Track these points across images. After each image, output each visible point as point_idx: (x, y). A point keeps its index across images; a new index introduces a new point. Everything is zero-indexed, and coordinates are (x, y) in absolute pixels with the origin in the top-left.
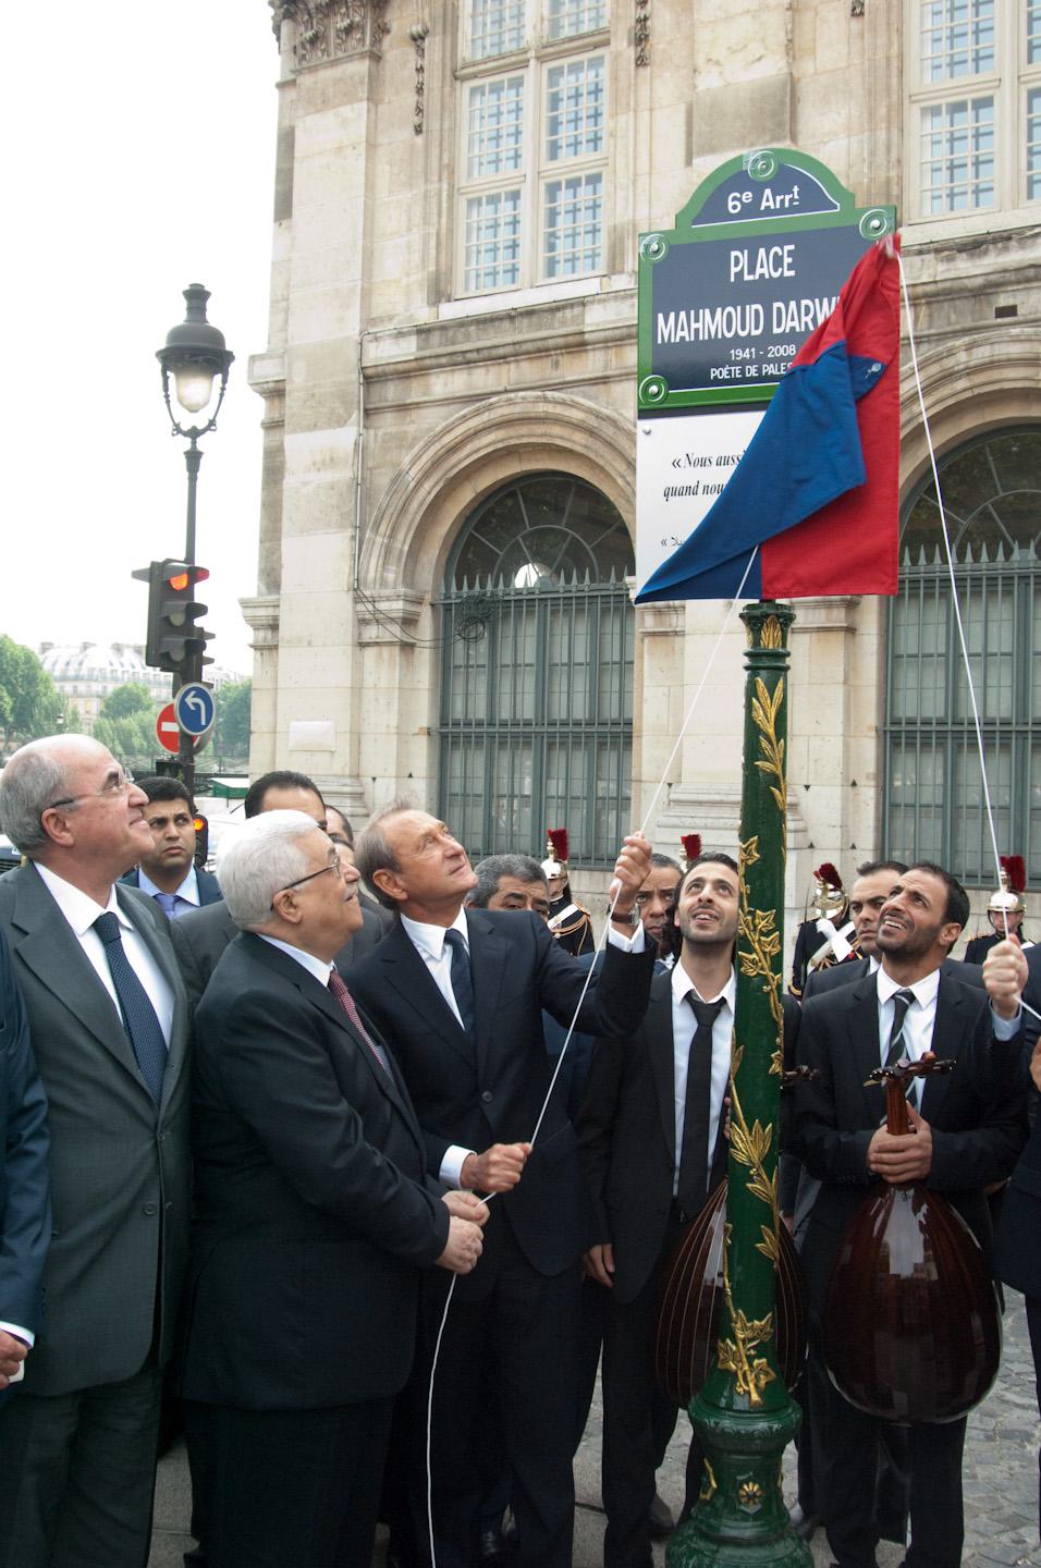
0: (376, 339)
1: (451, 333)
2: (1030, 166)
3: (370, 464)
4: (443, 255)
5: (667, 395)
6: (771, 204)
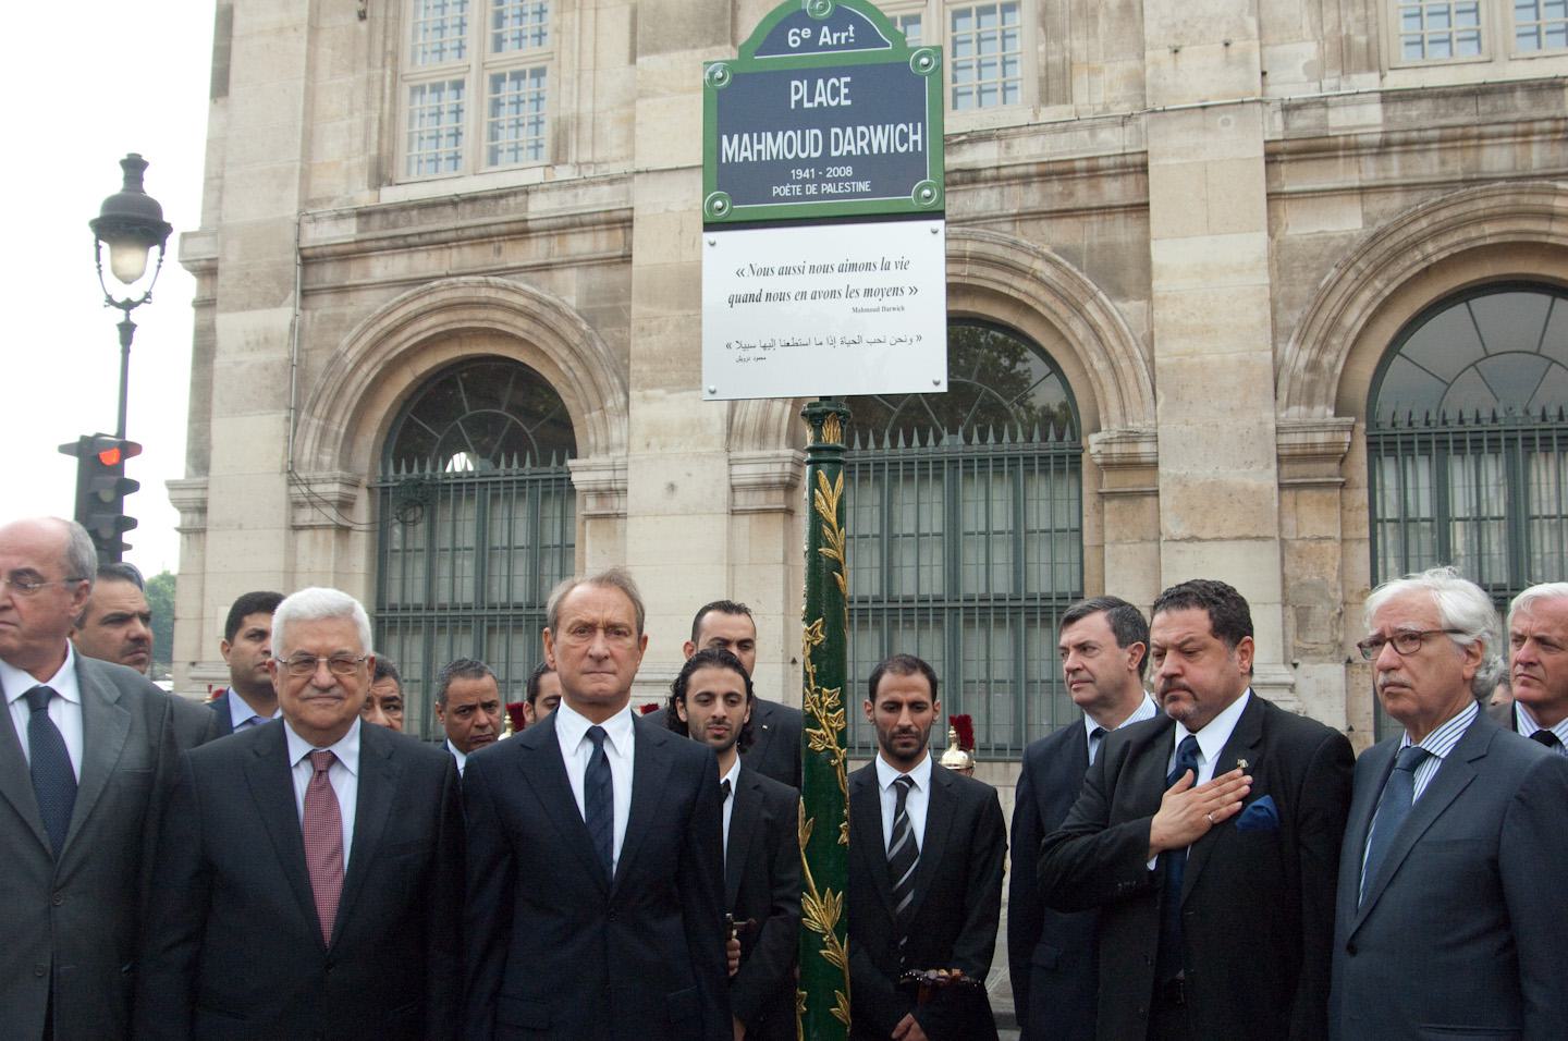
0: (315, 220)
1: (392, 217)
2: (955, 80)
3: (306, 346)
4: (385, 141)
5: (731, 210)
6: (828, 40)
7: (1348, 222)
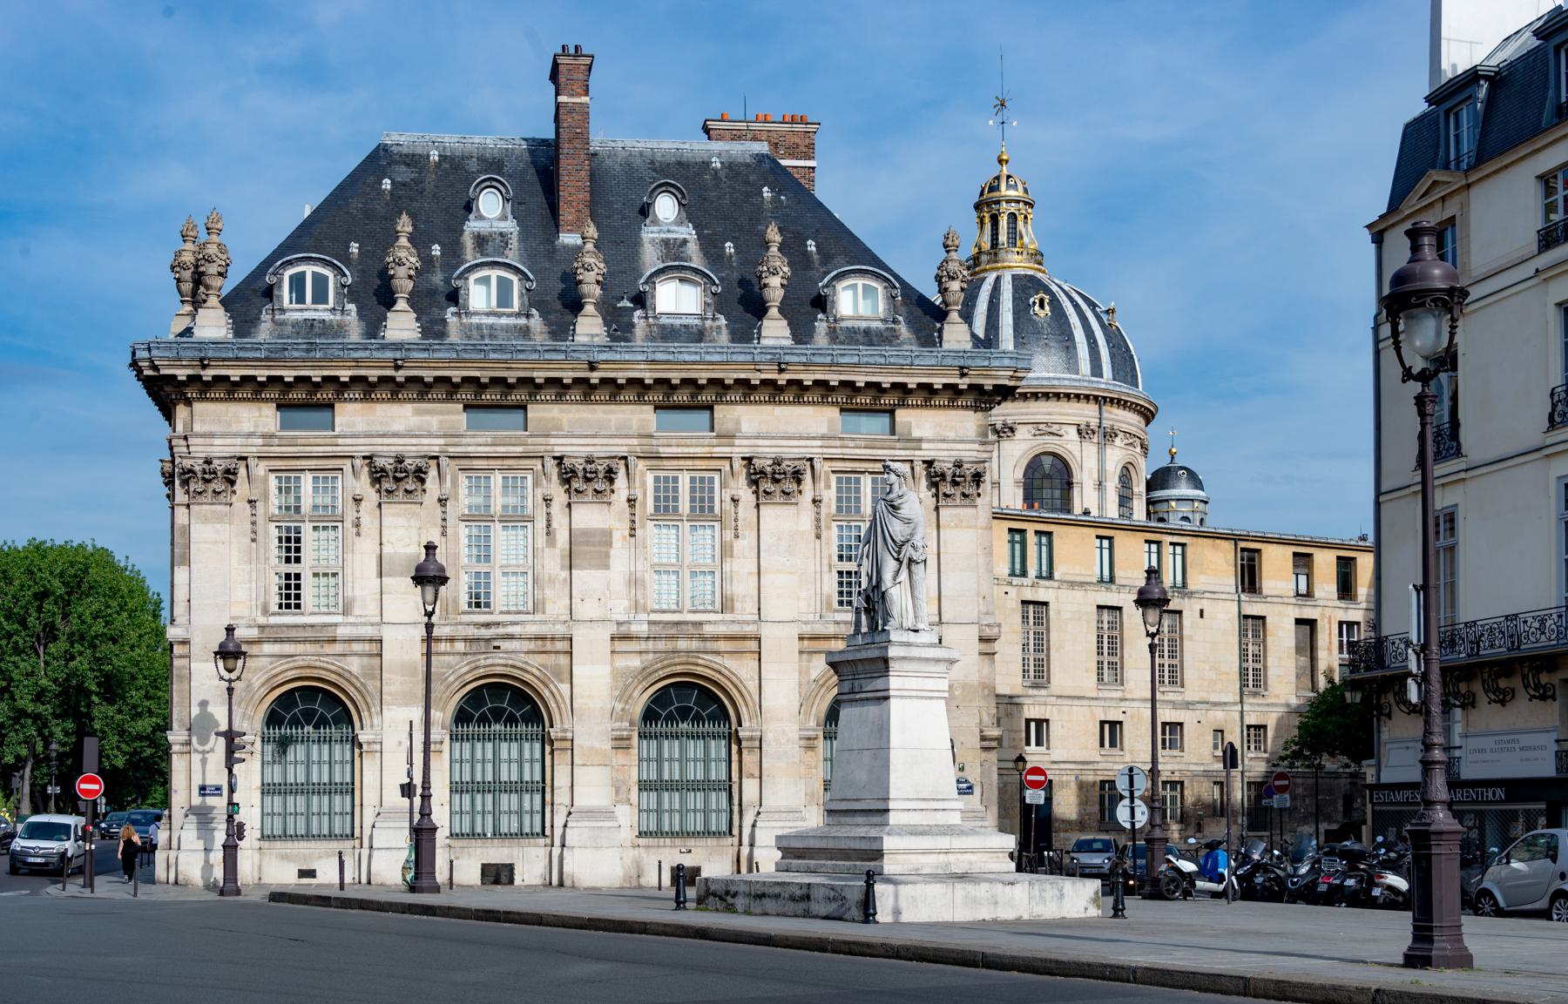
7: (635, 662)
